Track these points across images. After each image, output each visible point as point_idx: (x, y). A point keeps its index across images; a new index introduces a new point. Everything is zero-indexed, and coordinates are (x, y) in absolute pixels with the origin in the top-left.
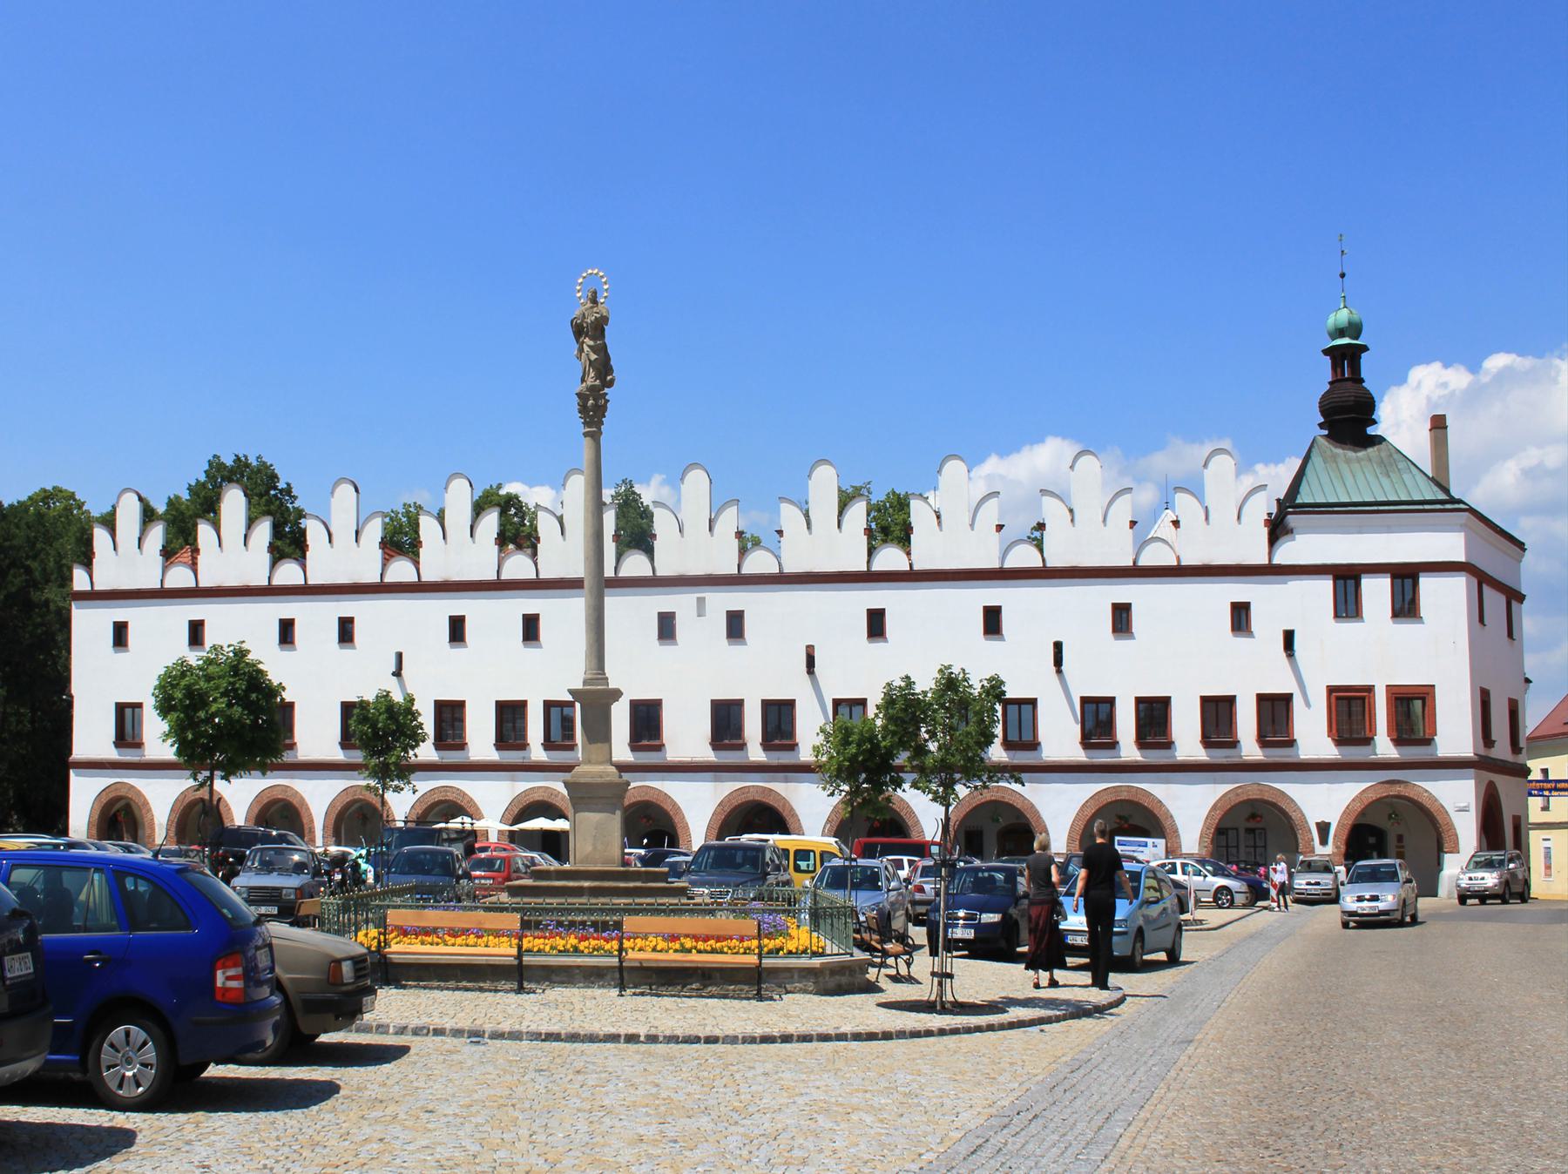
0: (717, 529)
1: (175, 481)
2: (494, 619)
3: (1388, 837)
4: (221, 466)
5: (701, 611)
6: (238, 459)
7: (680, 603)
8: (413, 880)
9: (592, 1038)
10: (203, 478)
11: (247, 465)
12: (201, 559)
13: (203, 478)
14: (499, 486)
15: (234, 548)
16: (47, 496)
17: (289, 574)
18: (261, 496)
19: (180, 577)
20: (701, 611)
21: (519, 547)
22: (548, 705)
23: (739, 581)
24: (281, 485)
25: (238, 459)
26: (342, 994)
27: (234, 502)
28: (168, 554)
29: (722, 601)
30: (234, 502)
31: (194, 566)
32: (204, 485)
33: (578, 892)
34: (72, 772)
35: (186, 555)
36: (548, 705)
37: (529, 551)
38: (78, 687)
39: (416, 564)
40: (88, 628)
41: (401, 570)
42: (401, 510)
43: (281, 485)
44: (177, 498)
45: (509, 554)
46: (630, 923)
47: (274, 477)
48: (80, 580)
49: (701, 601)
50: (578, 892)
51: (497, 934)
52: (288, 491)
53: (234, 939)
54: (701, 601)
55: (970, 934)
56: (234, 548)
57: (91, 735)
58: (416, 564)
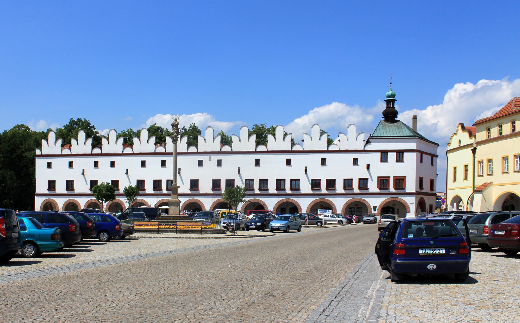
0: (215, 141)
1: (61, 124)
2: (153, 162)
3: (288, 209)
4: (73, 121)
5: (210, 159)
6: (78, 119)
7: (205, 158)
8: (136, 218)
9: (170, 238)
10: (68, 124)
11: (81, 121)
12: (72, 148)
13: (68, 124)
14: (155, 124)
15: (81, 144)
16: (19, 127)
17: (97, 151)
18: (85, 128)
19: (66, 151)
20: (210, 159)
21: (161, 145)
22: (168, 181)
23: (221, 153)
24: (91, 126)
25: (78, 119)
26: (130, 231)
27: (82, 135)
28: (63, 146)
29: (215, 158)
30: (82, 135)
31: (70, 149)
32: (68, 126)
33: (170, 219)
34: (36, 197)
35: (67, 146)
36: (168, 181)
37: (163, 145)
38: (37, 176)
39: (132, 149)
40: (40, 164)
41: (128, 150)
42: (126, 130)
43: (91, 126)
44: (61, 129)
45: (158, 147)
46: (178, 223)
47: (89, 124)
48: (38, 152)
49: (210, 158)
50: (170, 219)
51: (154, 225)
52: (93, 127)
53: (117, 223)
54: (210, 158)
55: (254, 227)
56: (81, 144)
57: (41, 187)
58: (132, 149)
